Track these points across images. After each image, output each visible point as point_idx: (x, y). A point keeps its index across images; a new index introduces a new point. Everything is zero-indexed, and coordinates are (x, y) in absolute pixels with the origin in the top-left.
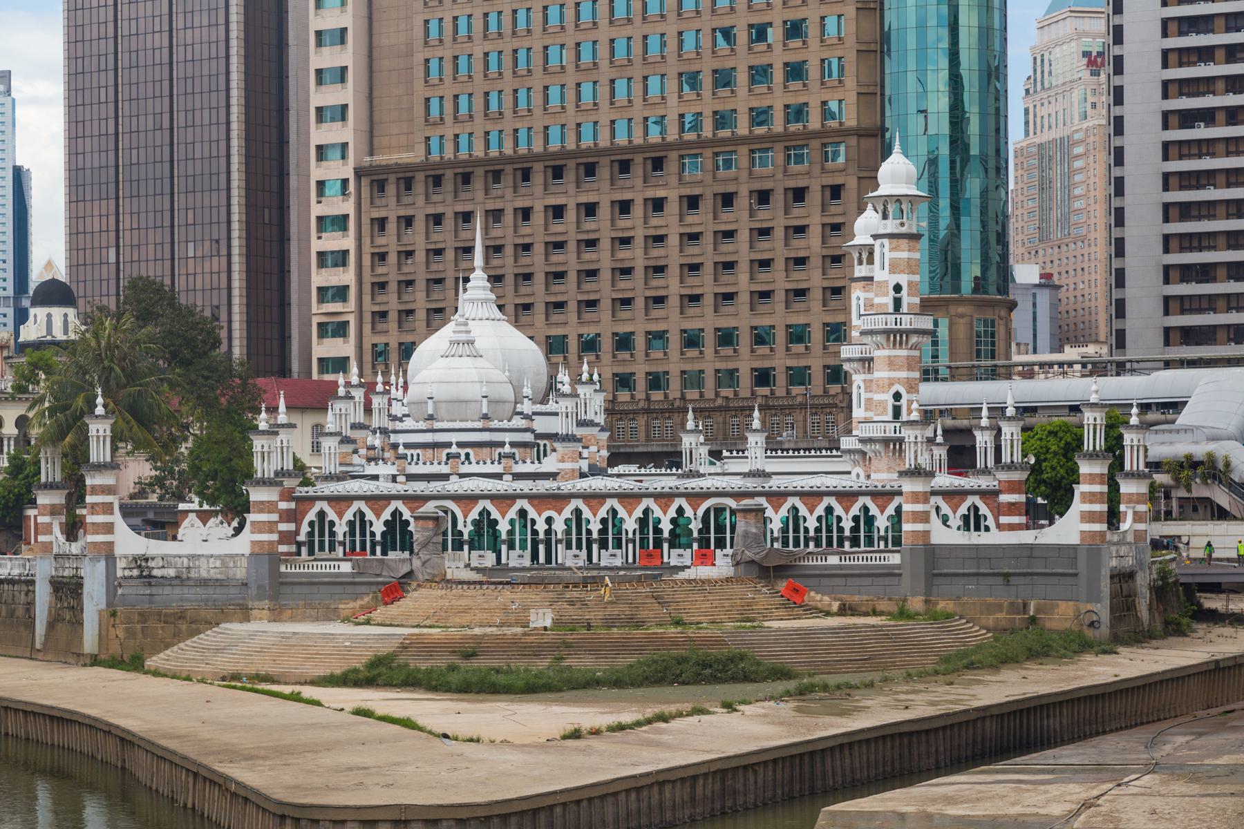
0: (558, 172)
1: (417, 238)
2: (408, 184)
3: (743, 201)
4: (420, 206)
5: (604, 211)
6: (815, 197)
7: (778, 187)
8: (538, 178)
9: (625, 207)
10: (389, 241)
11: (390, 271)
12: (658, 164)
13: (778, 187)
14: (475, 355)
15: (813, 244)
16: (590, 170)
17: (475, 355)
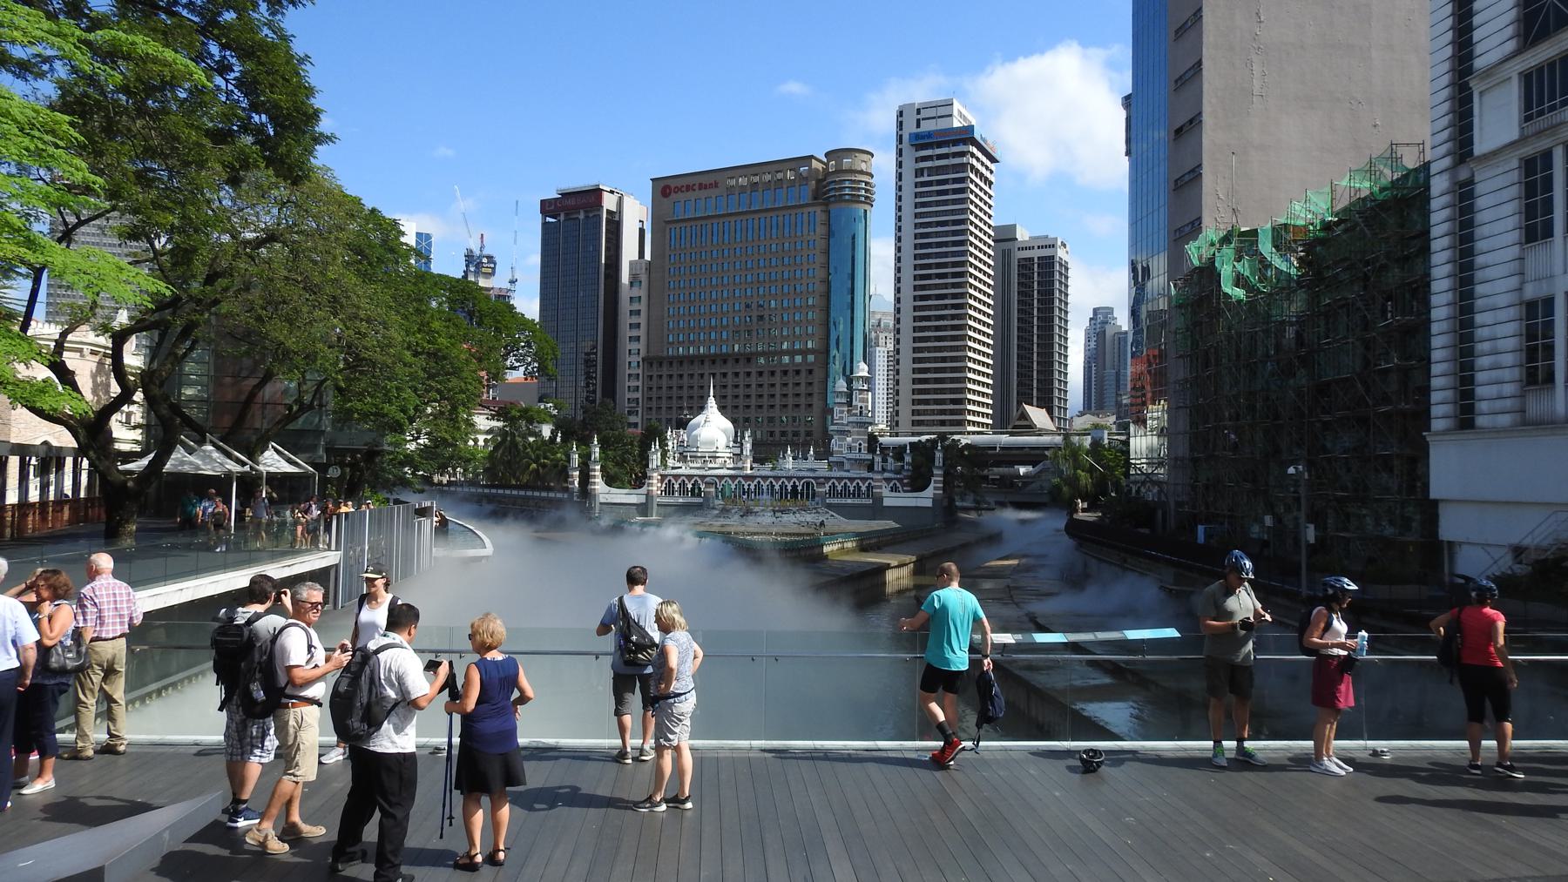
0: (714, 362)
1: (665, 382)
2: (661, 364)
3: (778, 374)
4: (665, 371)
5: (730, 376)
6: (803, 374)
7: (791, 369)
8: (707, 364)
9: (737, 374)
10: (654, 383)
11: (654, 394)
12: (749, 360)
13: (791, 369)
14: (713, 428)
15: (802, 389)
16: (725, 362)
17: (713, 428)
